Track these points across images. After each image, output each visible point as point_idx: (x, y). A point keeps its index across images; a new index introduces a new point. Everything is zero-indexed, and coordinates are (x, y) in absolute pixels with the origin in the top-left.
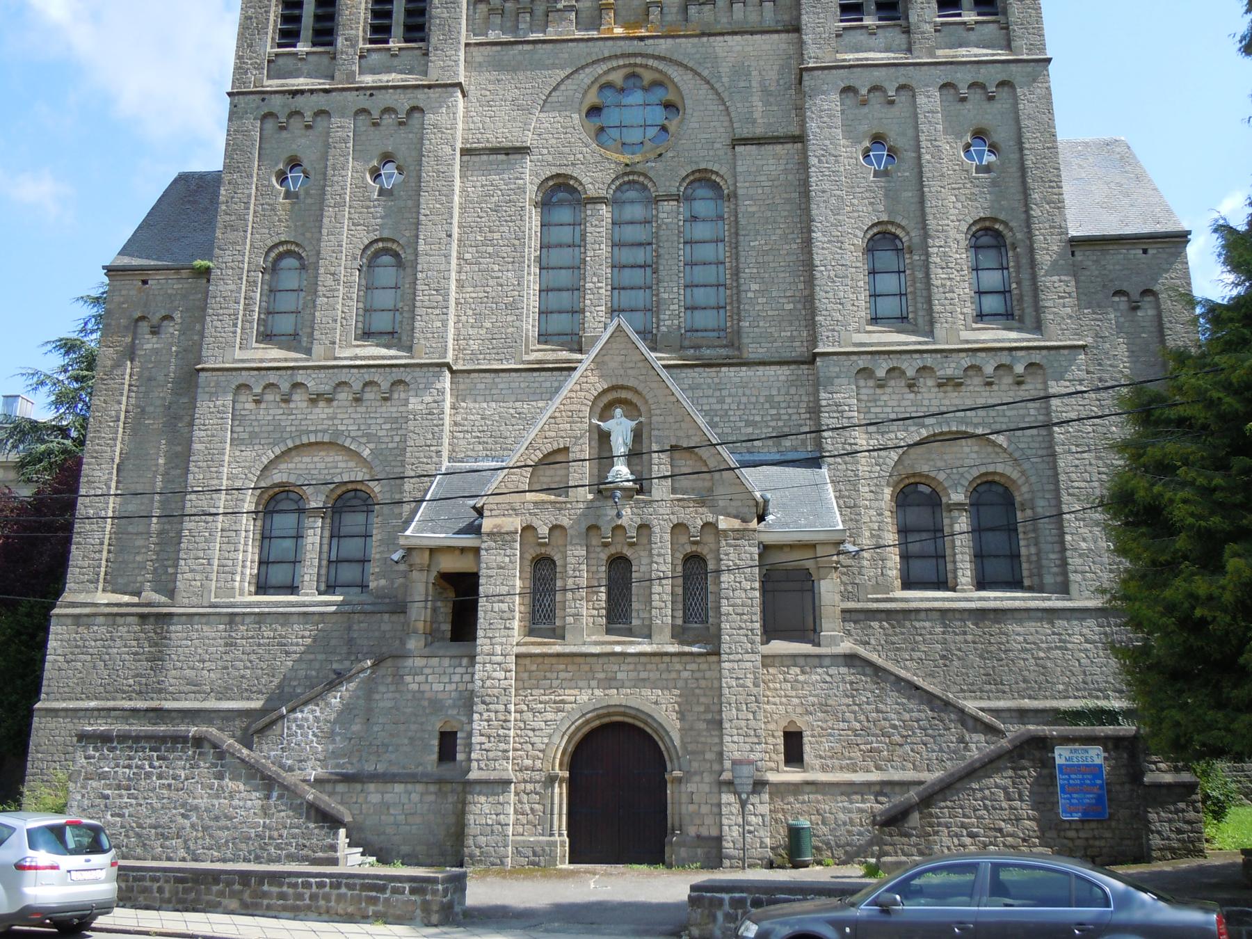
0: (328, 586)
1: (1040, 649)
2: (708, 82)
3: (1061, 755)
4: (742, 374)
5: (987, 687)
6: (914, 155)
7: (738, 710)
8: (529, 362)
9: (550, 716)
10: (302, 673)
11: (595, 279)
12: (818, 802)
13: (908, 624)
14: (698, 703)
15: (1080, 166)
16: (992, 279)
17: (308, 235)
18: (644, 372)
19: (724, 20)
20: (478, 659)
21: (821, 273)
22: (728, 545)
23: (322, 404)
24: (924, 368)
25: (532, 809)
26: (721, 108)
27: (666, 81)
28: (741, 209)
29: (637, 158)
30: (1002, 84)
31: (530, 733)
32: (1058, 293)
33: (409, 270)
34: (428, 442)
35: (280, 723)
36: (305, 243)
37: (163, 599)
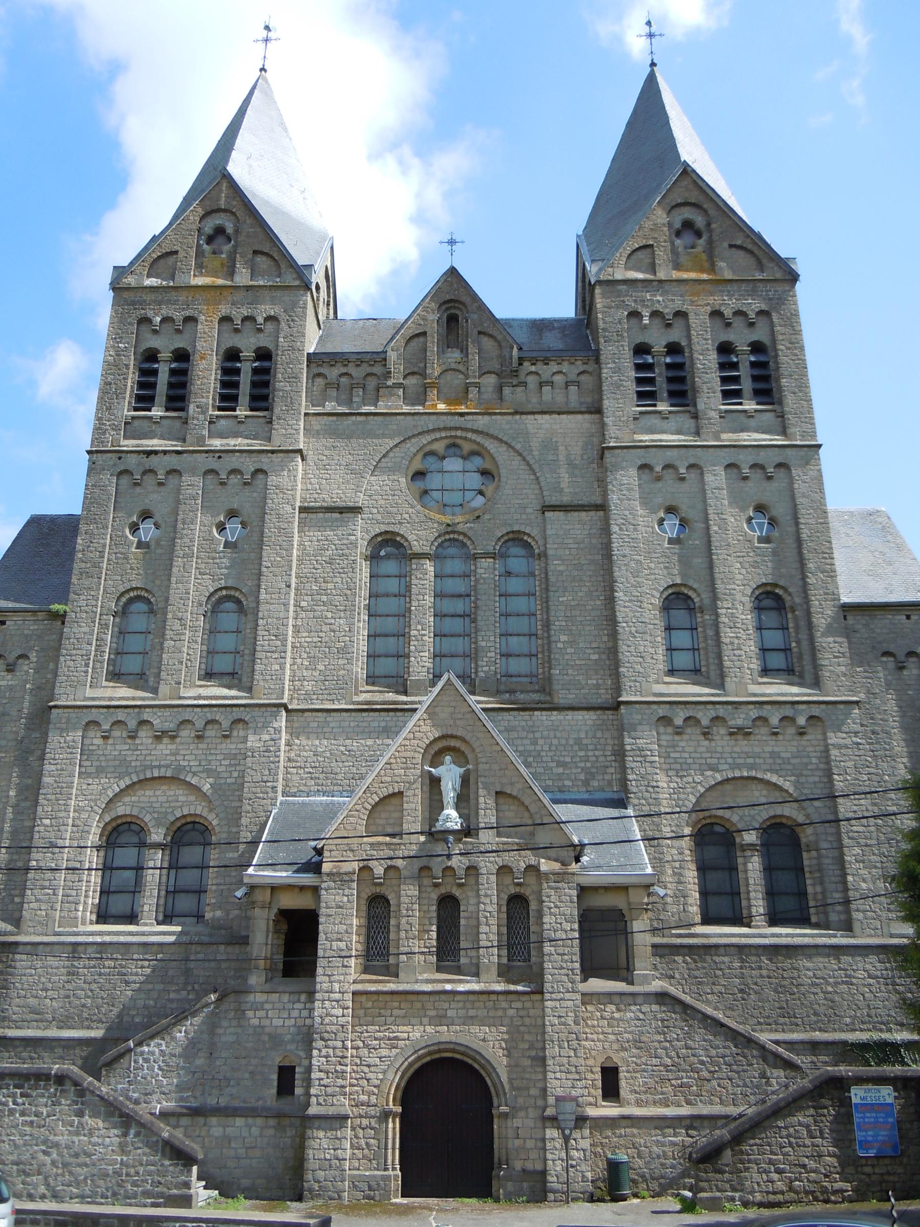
0: (165, 916)
1: (828, 983)
2: (520, 455)
3: (857, 1094)
4: (553, 718)
5: (782, 1020)
6: (703, 526)
7: (560, 1047)
8: (359, 703)
9: (384, 1052)
10: (140, 1003)
11: (419, 627)
12: (634, 1136)
13: (708, 958)
14: (523, 1040)
15: (848, 535)
16: (775, 638)
17: (158, 582)
18: (471, 722)
19: (534, 400)
20: (318, 996)
21: (624, 628)
22: (549, 887)
23: (166, 740)
24: (717, 718)
25: (367, 1144)
26: (532, 477)
27: (483, 452)
28: (551, 568)
29: (459, 519)
30: (780, 465)
31: (366, 1069)
32: (833, 652)
33: (250, 617)
34: (265, 778)
35: (127, 1057)
36: (155, 590)
37: (9, 928)
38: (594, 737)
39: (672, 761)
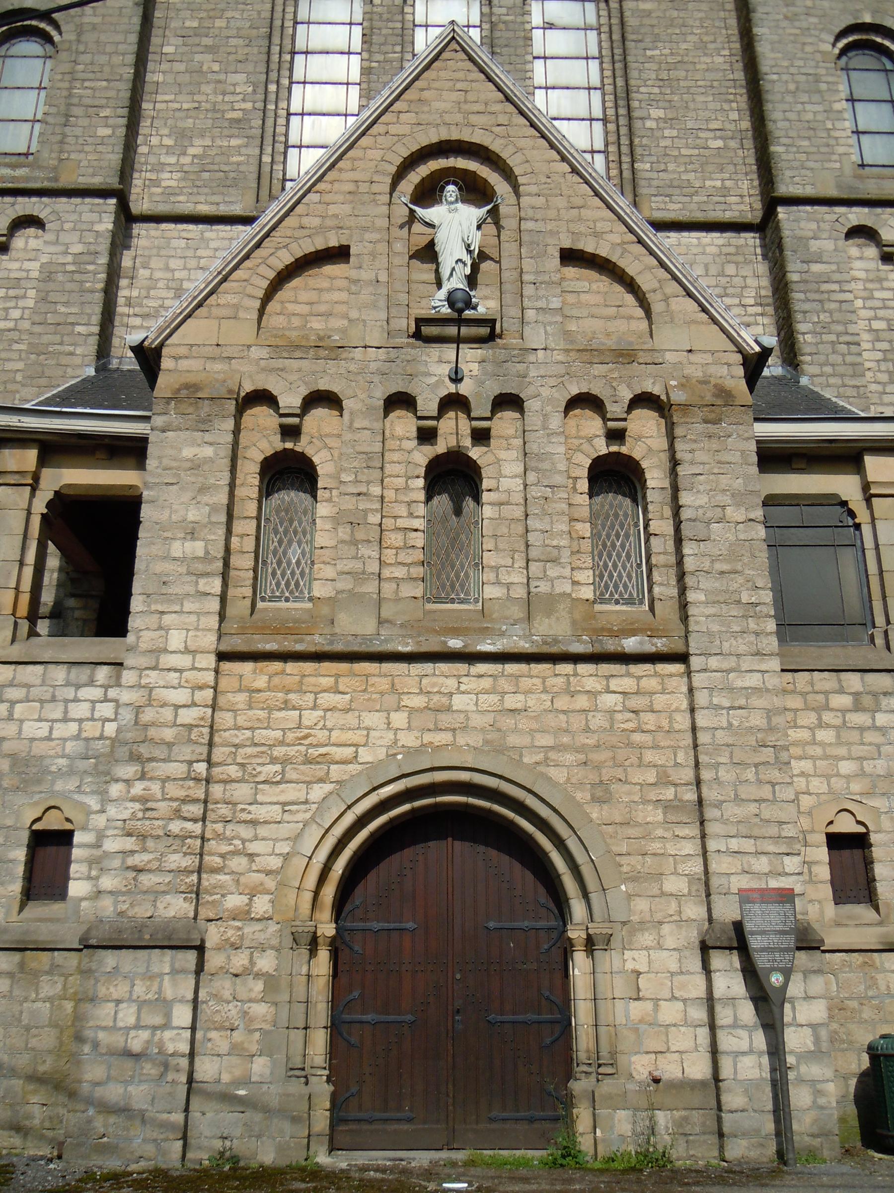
31: (245, 832)
38: (722, 274)
39: (879, 304)
